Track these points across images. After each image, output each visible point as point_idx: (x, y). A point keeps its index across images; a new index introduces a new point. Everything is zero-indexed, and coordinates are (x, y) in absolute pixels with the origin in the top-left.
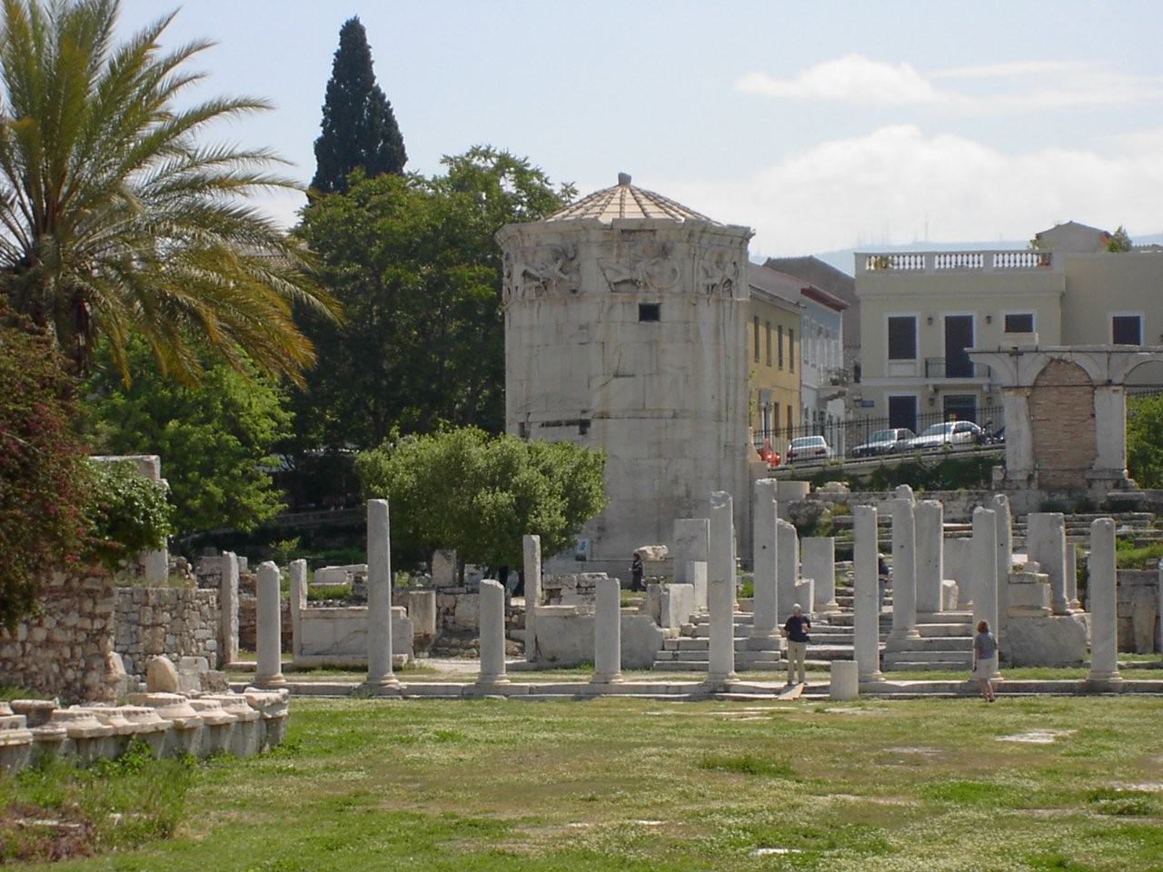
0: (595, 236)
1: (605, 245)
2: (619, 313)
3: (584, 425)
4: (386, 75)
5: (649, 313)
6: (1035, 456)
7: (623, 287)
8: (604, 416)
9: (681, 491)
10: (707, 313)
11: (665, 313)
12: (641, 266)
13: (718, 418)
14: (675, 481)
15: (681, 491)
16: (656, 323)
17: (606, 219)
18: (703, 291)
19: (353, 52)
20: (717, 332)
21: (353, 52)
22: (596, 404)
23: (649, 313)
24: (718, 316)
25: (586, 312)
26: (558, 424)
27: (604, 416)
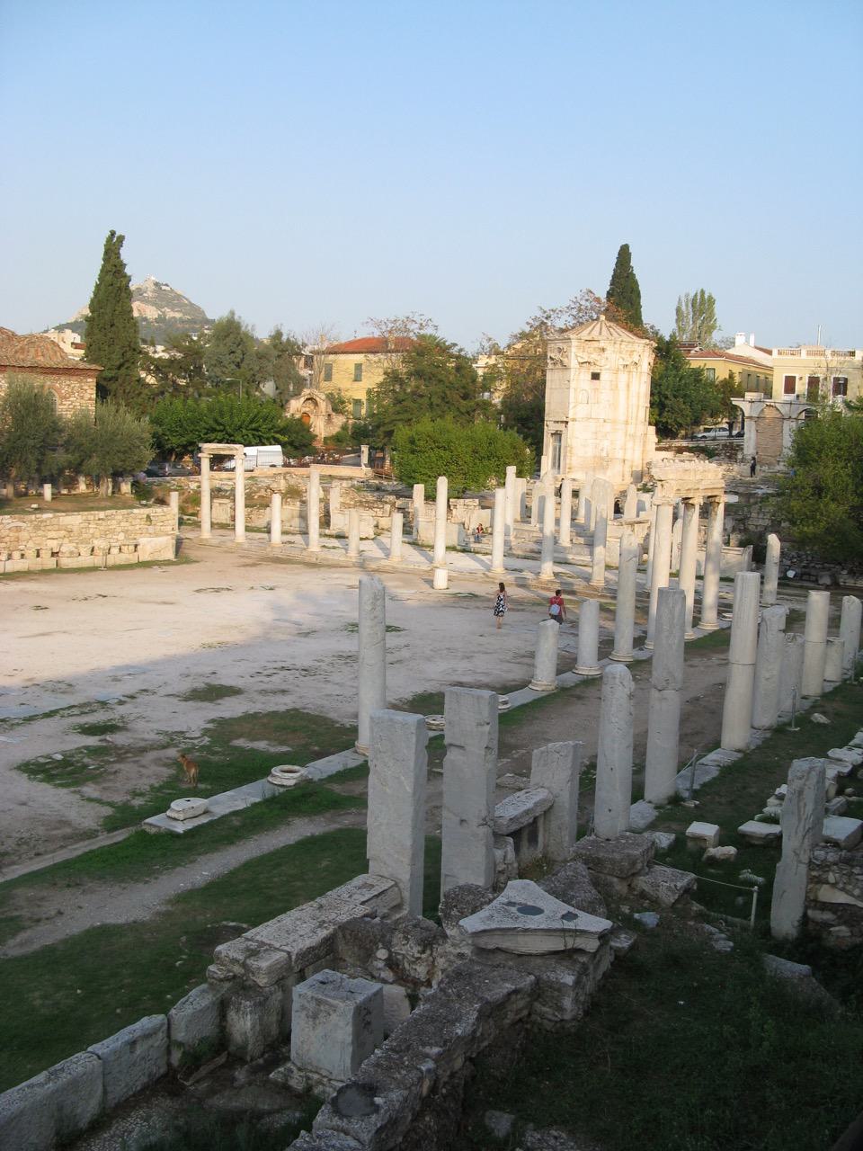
2: (582, 376)
3: (567, 422)
5: (596, 376)
7: (585, 365)
8: (574, 420)
9: (604, 454)
10: (623, 377)
11: (602, 377)
12: (592, 356)
13: (627, 423)
14: (602, 450)
15: (604, 454)
16: (597, 381)
18: (621, 367)
19: (624, 255)
20: (628, 386)
21: (624, 255)
23: (596, 376)
24: (629, 378)
26: (558, 422)
27: (574, 420)
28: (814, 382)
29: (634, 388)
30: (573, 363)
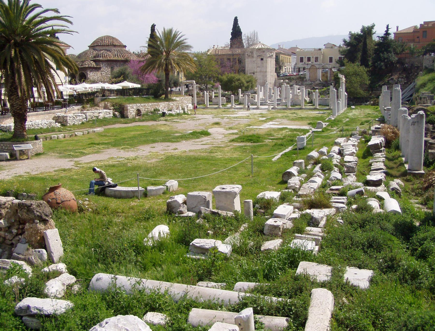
0: (255, 50)
1: (257, 51)
2: (258, 59)
3: (254, 73)
4: (240, 24)
5: (262, 59)
6: (310, 77)
8: (256, 72)
11: (264, 60)
17: (256, 48)
19: (236, 20)
21: (236, 20)
22: (255, 71)
23: (262, 59)
25: (254, 59)
27: (256, 72)
28: (309, 59)
29: (272, 62)
30: (255, 55)
